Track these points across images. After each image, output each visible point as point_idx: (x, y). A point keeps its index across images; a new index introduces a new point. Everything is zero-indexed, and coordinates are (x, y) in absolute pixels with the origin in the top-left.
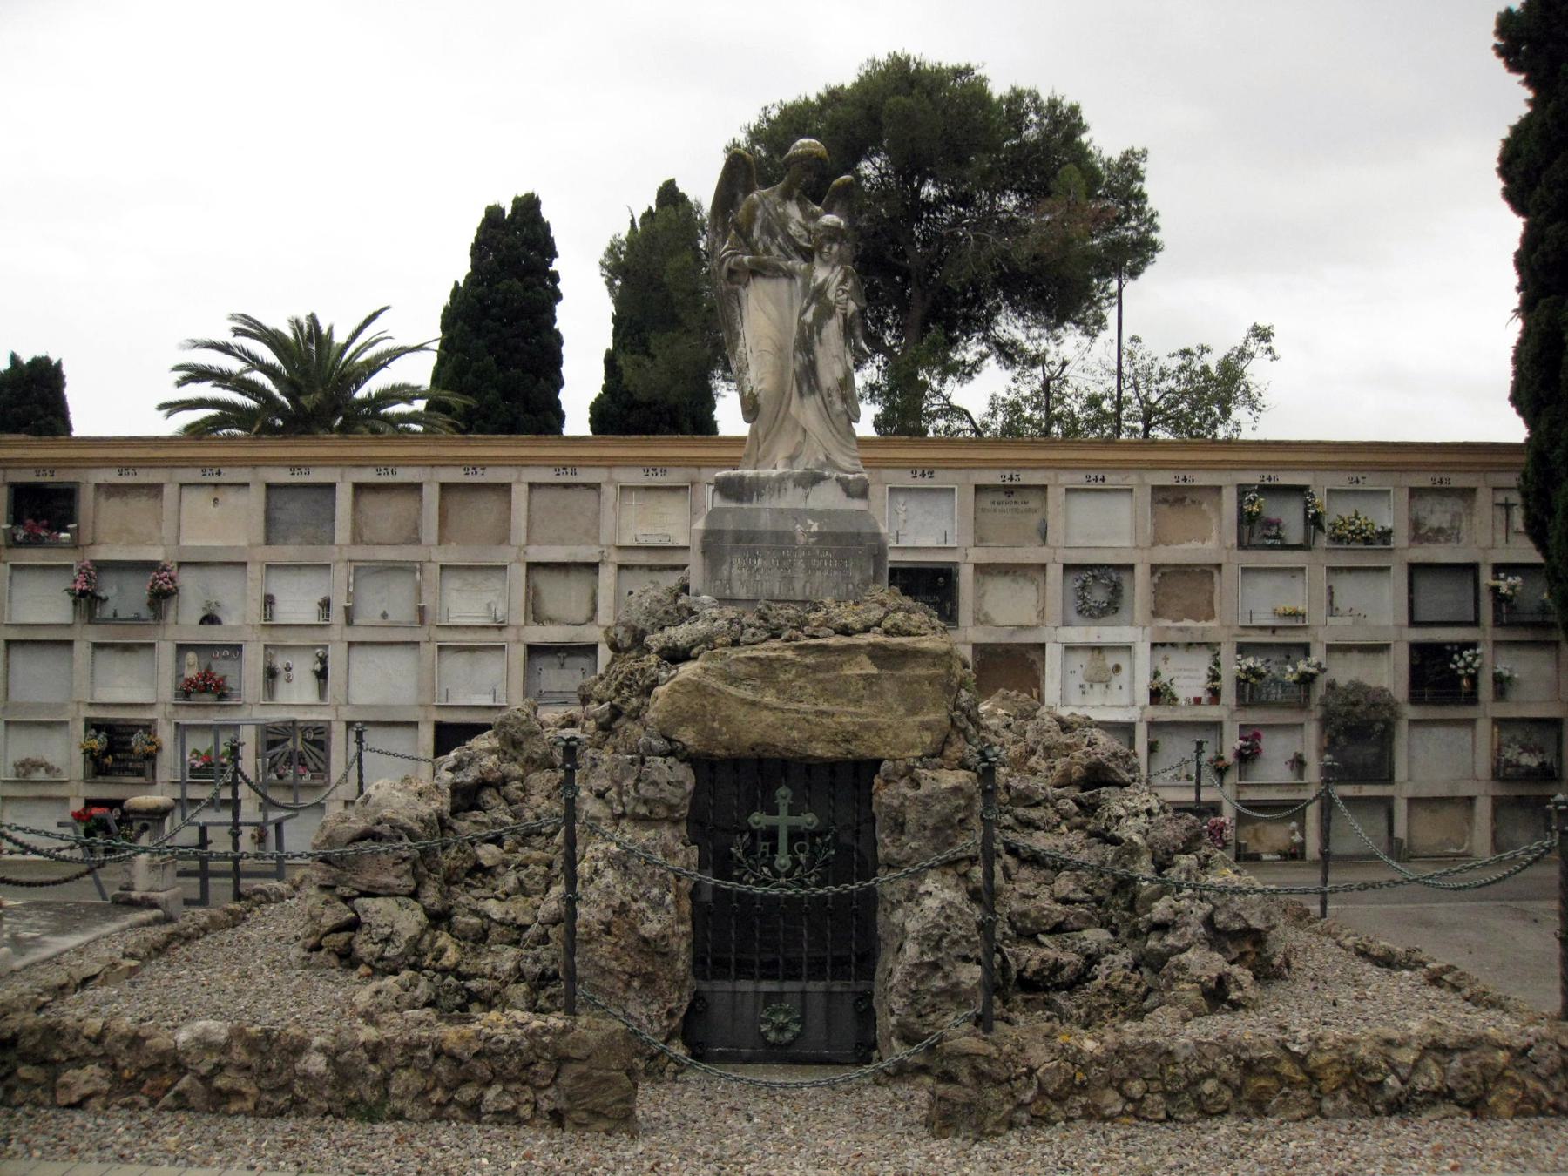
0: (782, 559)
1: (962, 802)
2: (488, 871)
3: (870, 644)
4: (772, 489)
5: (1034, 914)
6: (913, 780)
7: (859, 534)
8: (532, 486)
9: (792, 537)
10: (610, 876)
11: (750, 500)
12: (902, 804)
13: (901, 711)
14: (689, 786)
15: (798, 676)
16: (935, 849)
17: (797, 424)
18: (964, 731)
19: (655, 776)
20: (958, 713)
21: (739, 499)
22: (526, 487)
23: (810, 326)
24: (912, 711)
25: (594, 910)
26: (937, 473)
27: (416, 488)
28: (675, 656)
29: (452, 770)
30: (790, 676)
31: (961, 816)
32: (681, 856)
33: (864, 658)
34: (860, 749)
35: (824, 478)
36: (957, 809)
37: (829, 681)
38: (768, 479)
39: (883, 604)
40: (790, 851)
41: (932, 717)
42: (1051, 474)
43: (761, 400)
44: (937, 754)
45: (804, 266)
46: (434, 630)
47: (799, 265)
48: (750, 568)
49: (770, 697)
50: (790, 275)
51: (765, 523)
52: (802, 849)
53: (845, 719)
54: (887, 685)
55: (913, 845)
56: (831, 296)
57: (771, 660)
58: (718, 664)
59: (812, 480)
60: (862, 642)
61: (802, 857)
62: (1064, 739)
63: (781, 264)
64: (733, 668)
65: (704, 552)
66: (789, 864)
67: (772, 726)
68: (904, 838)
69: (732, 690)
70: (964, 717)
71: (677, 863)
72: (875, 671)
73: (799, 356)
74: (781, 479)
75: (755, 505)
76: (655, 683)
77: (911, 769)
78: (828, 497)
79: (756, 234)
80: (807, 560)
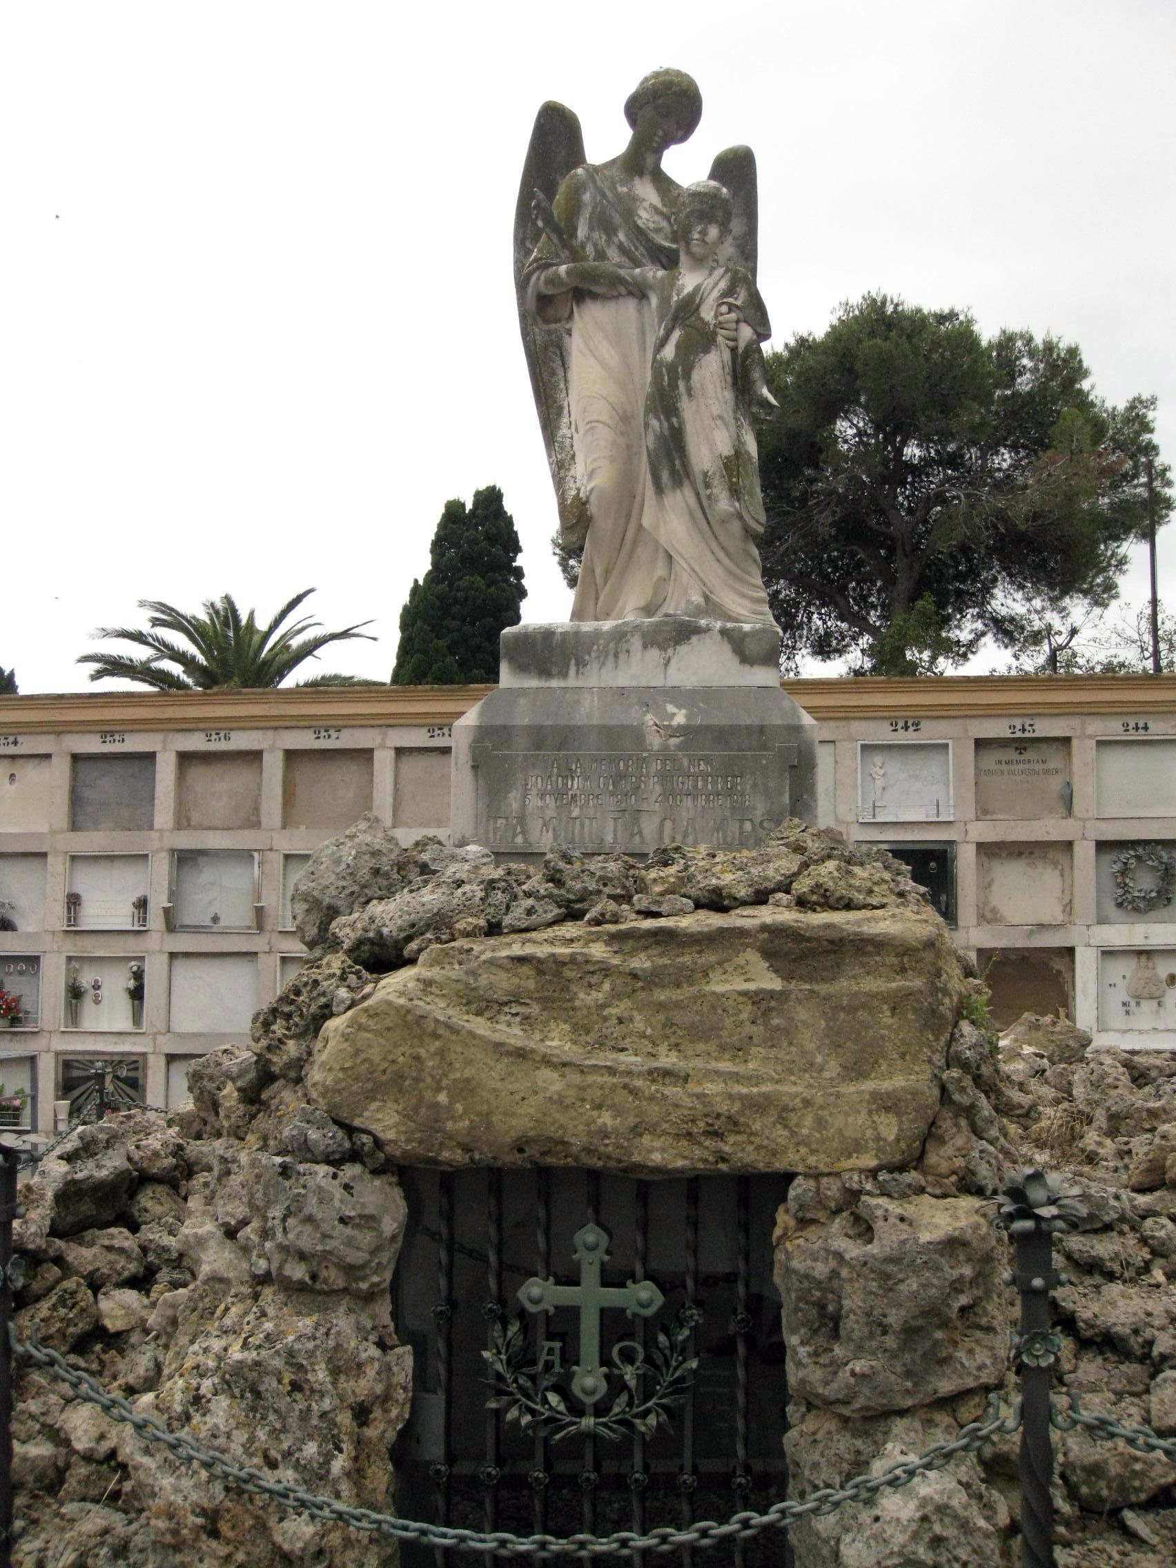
0: (619, 777)
1: (967, 1271)
2: (116, 1341)
3: (764, 928)
4: (602, 656)
5: (1114, 1469)
6: (857, 1219)
7: (762, 729)
8: (400, 751)
9: (636, 734)
10: (221, 1411)
11: (564, 675)
12: (835, 1274)
13: (833, 1068)
14: (390, 1225)
15: (616, 995)
16: (908, 1374)
17: (657, 544)
18: (969, 1111)
19: (312, 1206)
20: (955, 1073)
21: (545, 673)
22: (392, 753)
23: (672, 368)
24: (856, 1070)
25: (186, 1483)
26: (924, 724)
27: (254, 757)
28: (381, 957)
29: (69, 1158)
30: (598, 996)
31: (964, 1300)
32: (371, 1372)
33: (751, 956)
34: (744, 1153)
35: (698, 631)
36: (957, 1286)
37: (678, 1005)
38: (597, 634)
39: (799, 849)
40: (605, 1361)
41: (898, 1082)
42: (1075, 722)
43: (593, 509)
44: (909, 1164)
45: (661, 273)
46: (275, 936)
47: (654, 273)
48: (559, 794)
49: (557, 1041)
50: (640, 292)
51: (588, 712)
52: (628, 1357)
53: (711, 1088)
54: (802, 1014)
55: (859, 1366)
56: (707, 314)
57: (560, 963)
58: (456, 971)
59: (681, 632)
60: (747, 923)
61: (629, 1374)
62: (1141, 1099)
63: (622, 272)
64: (484, 980)
65: (475, 767)
66: (603, 1387)
67: (559, 1102)
68: (839, 1351)
69: (480, 1026)
70: (968, 1081)
71: (364, 1386)
72: (775, 984)
73: (654, 423)
74: (620, 635)
75: (572, 682)
76: (326, 1012)
77: (853, 1195)
78: (706, 665)
79: (582, 232)
80: (664, 777)
